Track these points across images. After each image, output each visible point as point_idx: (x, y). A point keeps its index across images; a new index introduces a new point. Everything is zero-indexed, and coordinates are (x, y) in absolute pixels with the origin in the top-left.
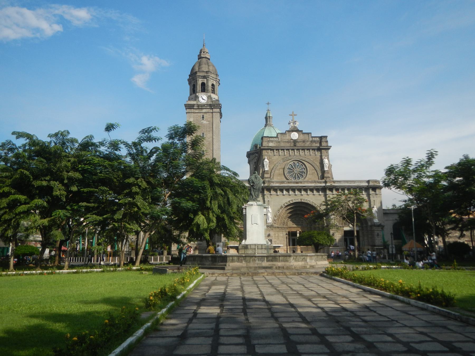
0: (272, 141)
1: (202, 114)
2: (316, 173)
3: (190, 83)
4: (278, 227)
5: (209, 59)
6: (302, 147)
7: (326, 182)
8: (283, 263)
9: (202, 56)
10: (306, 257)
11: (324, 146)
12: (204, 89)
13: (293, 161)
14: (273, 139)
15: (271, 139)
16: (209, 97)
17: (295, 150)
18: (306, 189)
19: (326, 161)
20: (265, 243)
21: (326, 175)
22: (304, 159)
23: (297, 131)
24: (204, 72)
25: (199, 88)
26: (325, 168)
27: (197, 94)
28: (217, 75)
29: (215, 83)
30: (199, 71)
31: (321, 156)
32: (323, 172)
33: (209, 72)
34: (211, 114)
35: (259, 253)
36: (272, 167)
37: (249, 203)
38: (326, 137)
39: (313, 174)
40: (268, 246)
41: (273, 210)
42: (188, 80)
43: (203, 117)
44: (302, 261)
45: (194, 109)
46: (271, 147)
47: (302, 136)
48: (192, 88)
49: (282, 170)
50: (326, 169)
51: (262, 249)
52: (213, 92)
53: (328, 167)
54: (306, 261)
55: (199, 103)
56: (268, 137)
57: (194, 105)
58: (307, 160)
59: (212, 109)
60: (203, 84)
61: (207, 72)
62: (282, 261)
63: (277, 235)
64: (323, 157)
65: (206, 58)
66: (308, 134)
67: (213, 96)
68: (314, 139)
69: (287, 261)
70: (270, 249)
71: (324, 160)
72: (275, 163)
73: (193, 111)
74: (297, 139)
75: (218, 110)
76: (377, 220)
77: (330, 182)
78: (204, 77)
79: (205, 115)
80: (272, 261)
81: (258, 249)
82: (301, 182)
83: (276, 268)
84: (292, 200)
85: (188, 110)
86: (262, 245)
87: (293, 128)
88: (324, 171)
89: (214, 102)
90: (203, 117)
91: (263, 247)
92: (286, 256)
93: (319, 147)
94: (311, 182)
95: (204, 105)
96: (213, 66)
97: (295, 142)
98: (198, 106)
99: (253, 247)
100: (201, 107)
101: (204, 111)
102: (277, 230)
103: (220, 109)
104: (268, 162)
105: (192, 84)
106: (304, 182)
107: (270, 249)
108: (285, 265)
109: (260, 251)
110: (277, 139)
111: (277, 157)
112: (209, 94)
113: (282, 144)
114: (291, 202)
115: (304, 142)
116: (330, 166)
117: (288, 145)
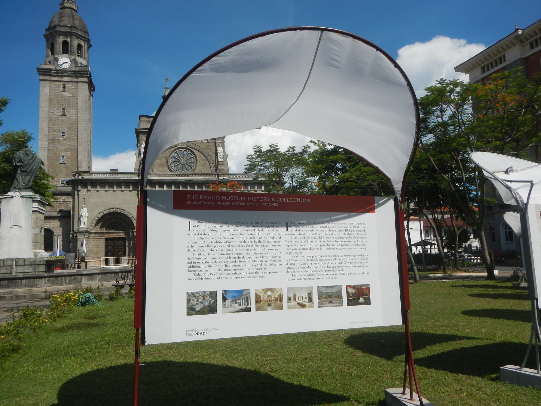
1: (61, 84)
3: (47, 41)
5: (76, 11)
7: (218, 176)
8: (27, 289)
9: (66, 5)
10: (79, 277)
12: (66, 50)
16: (74, 61)
19: (220, 149)
20: (32, 256)
21: (219, 167)
22: (193, 146)
24: (65, 26)
25: (59, 47)
27: (56, 56)
28: (86, 33)
29: (82, 43)
30: (59, 26)
31: (215, 144)
32: (217, 163)
33: (74, 27)
34: (76, 83)
35: (17, 271)
37: (9, 193)
39: (204, 165)
40: (35, 261)
42: (45, 36)
43: (64, 88)
44: (70, 282)
45: (50, 75)
48: (50, 46)
50: (220, 159)
51: (24, 265)
52: (80, 55)
53: (223, 158)
54: (80, 282)
55: (59, 68)
57: (50, 70)
58: (198, 148)
59: (77, 77)
60: (65, 43)
61: (71, 27)
62: (25, 286)
64: (218, 145)
65: (71, 8)
67: (79, 60)
69: (34, 286)
70: (39, 265)
71: (218, 148)
73: (48, 78)
75: (86, 80)
77: (224, 174)
78: (66, 34)
79: (67, 85)
80: (8, 287)
81: (17, 265)
82: (187, 175)
83: (12, 298)
85: (42, 77)
86: (24, 260)
88: (218, 162)
89: (80, 68)
90: (64, 88)
91: (27, 263)
92: (34, 278)
95: (65, 71)
96: (81, 21)
98: (57, 71)
99: (9, 263)
100: (62, 73)
101: (65, 79)
103: (90, 77)
105: (50, 42)
107: (39, 265)
108: (30, 292)
109: (20, 269)
112: (73, 57)
116: (225, 156)
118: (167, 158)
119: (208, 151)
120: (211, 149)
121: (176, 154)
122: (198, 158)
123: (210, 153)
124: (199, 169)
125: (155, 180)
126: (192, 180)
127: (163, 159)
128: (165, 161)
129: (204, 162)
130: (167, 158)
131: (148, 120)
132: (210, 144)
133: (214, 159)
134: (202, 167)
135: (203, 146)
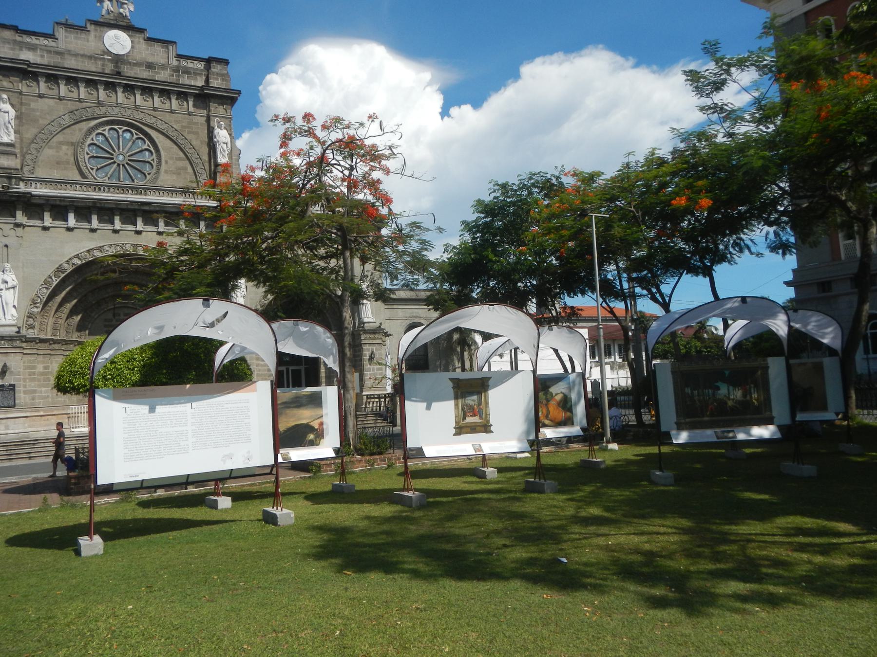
0: (33, 48)
2: (190, 169)
4: (42, 341)
6: (143, 80)
11: (217, 89)
13: (112, 122)
14: (33, 40)
15: (27, 39)
17: (120, 91)
18: (149, 213)
19: (222, 135)
21: (221, 179)
22: (150, 120)
23: (129, 28)
26: (219, 154)
31: (208, 119)
36: (29, 134)
38: (226, 62)
39: (178, 172)
41: (24, 281)
46: (28, 63)
47: (142, 45)
49: (66, 152)
50: (222, 159)
53: (230, 155)
56: (15, 29)
58: (161, 126)
63: (40, 368)
64: (214, 123)
66: (166, 43)
68: (184, 63)
71: (217, 131)
72: (43, 122)
74: (127, 55)
76: (370, 315)
82: (137, 190)
84: (100, 249)
87: (112, 16)
88: (217, 165)
93: (202, 88)
94: (172, 192)
97: (118, 59)
102: (44, 348)
104: (13, 113)
106: (145, 190)
110: (54, 44)
111: (51, 102)
113: (71, 63)
114: (98, 254)
115: (150, 66)
117: (91, 66)
118: (76, 146)
119: (189, 137)
120: (196, 133)
121: (101, 138)
122: (163, 153)
123: (194, 143)
124: (166, 179)
125: (40, 196)
126: (149, 204)
127: (64, 147)
128: (70, 152)
129: (181, 164)
130: (76, 146)
131: (18, 39)
132: (196, 119)
133: (205, 158)
134: (175, 177)
135: (177, 122)
